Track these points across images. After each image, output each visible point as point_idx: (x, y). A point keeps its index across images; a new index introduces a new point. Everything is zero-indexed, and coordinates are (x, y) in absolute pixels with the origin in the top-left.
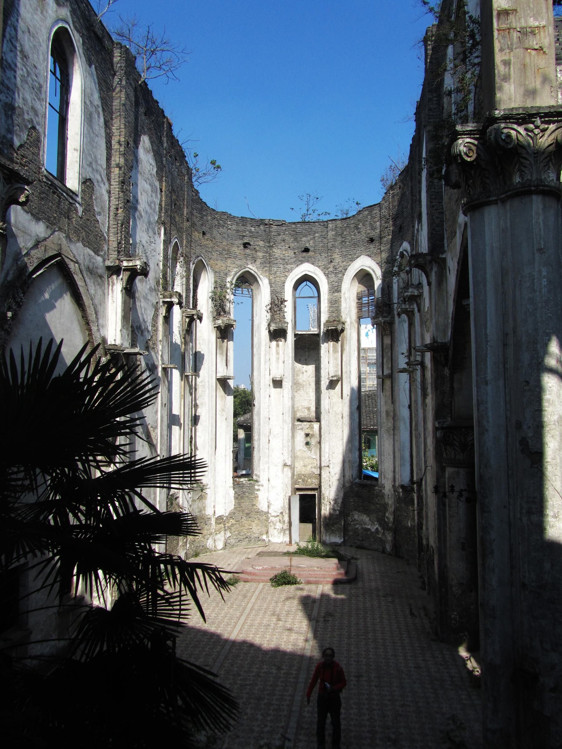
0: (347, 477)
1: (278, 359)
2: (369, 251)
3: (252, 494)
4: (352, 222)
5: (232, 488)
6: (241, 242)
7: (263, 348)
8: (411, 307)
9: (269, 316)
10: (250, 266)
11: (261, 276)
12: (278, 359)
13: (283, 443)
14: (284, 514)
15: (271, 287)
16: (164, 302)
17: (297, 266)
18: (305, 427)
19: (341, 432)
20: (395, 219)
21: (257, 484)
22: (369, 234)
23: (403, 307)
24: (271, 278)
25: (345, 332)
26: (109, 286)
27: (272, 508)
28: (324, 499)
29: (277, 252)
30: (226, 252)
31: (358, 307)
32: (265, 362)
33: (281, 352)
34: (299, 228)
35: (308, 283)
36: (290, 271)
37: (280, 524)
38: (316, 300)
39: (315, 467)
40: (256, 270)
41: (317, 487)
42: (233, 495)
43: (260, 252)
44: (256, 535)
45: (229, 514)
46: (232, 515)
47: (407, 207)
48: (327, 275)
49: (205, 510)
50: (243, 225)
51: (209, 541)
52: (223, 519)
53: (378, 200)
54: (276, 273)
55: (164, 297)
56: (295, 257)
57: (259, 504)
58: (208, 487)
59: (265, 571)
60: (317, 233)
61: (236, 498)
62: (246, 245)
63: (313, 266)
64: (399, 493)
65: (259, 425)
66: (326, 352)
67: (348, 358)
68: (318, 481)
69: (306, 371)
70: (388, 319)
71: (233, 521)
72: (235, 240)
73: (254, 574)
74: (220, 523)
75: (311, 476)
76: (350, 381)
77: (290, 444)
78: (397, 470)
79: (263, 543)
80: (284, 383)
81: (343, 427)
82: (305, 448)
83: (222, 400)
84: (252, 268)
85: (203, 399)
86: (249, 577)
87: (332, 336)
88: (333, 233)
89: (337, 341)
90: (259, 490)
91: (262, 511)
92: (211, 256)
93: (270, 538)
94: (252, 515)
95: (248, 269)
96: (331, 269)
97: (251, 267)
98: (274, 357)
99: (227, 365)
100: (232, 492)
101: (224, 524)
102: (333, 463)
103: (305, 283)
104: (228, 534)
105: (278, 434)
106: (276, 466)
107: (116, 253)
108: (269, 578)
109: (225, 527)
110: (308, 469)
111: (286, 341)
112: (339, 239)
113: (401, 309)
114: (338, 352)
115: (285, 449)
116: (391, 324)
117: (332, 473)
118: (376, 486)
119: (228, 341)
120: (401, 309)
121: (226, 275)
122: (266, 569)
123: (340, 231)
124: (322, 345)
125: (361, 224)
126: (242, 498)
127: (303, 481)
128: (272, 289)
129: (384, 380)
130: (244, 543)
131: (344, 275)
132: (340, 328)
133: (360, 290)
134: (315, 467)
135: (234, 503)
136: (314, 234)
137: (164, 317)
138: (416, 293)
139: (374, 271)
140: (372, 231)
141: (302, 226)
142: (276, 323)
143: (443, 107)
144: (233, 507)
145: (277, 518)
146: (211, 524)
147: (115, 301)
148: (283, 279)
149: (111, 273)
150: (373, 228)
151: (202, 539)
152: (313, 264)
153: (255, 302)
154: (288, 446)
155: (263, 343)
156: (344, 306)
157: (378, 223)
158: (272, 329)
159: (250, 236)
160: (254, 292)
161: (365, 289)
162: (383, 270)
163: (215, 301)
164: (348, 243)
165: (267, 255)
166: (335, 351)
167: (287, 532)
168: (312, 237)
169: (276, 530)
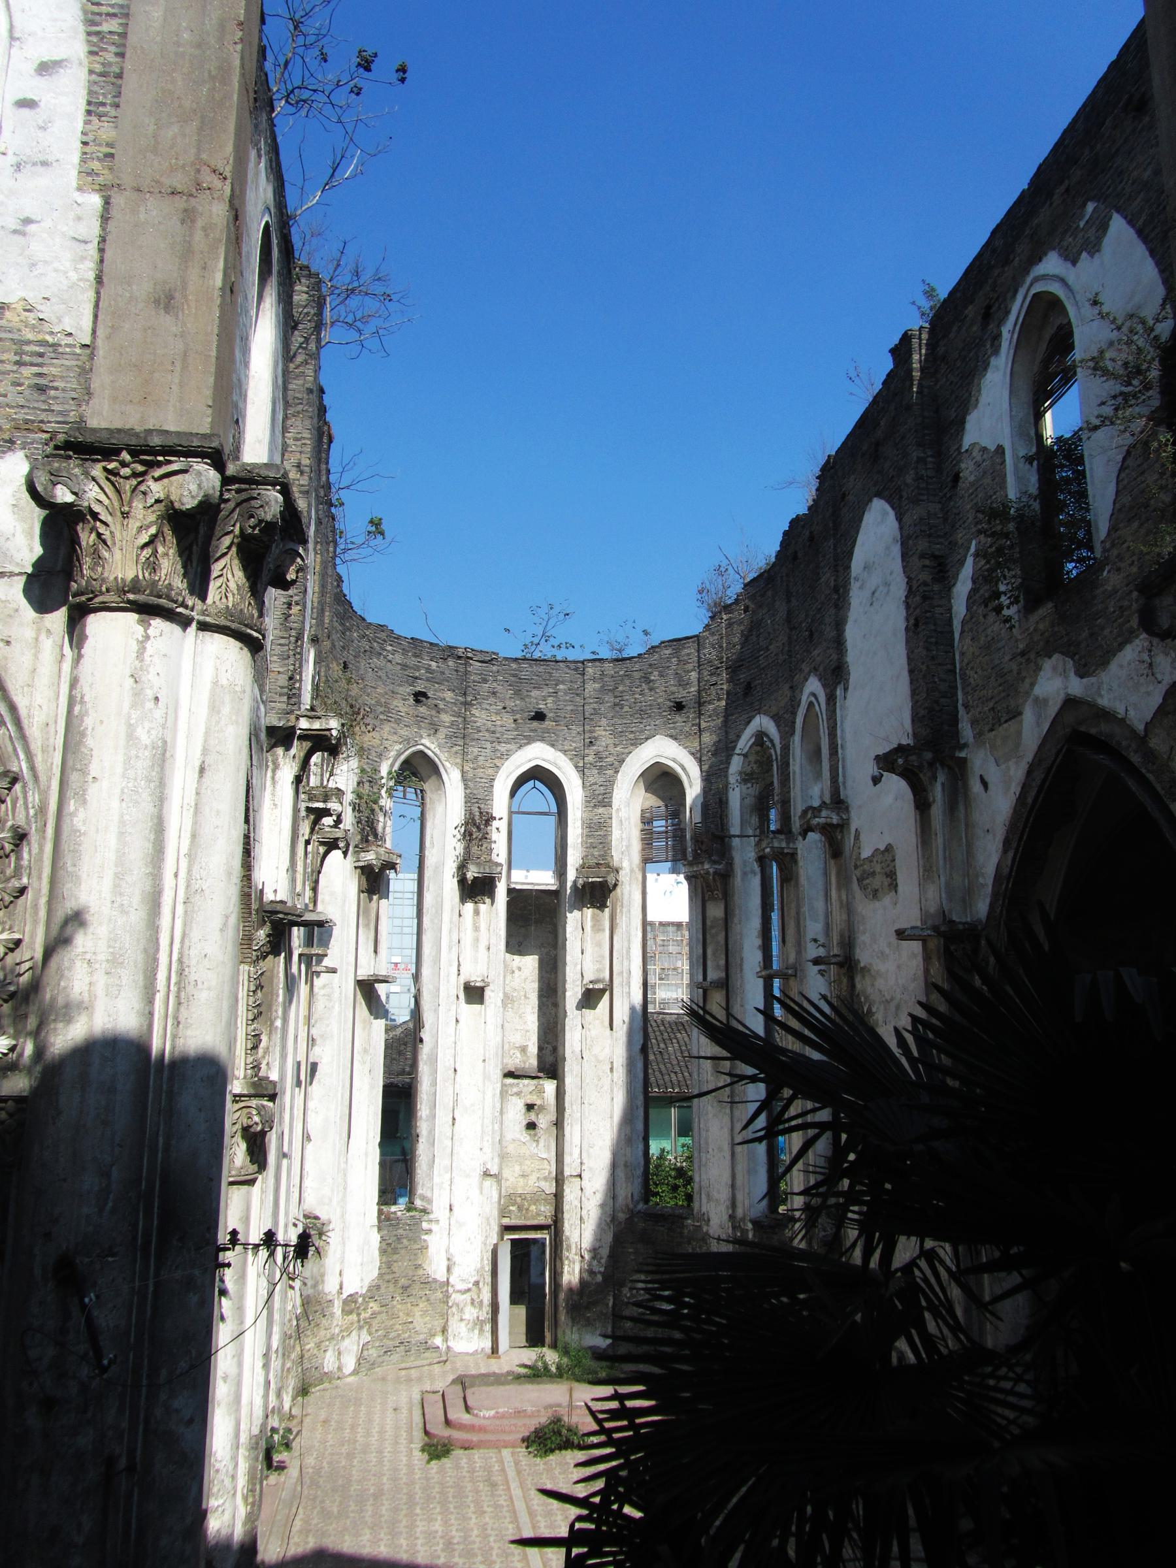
0: (620, 1200)
1: (477, 940)
2: (674, 728)
3: (415, 1242)
4: (637, 667)
5: (376, 1229)
6: (409, 689)
7: (446, 917)
8: (791, 845)
9: (460, 848)
10: (426, 741)
12: (477, 940)
13: (482, 1126)
14: (481, 1284)
15: (466, 787)
16: (309, 809)
17: (520, 747)
18: (525, 1090)
19: (609, 1100)
20: (734, 669)
21: (425, 1218)
22: (673, 693)
23: (776, 844)
25: (618, 889)
26: (267, 770)
27: (456, 1271)
28: (569, 1248)
29: (480, 716)
30: (381, 709)
31: (643, 840)
32: (450, 948)
33: (483, 926)
34: (526, 670)
35: (539, 784)
36: (506, 756)
37: (472, 1309)
38: (552, 821)
39: (545, 1179)
40: (437, 751)
41: (550, 1222)
42: (378, 1245)
43: (446, 713)
44: (422, 1337)
45: (368, 1291)
46: (374, 1291)
47: (767, 649)
48: (582, 771)
49: (323, 1282)
50: (415, 656)
51: (329, 1354)
52: (356, 1302)
53: (696, 628)
54: (476, 758)
55: (310, 800)
56: (516, 730)
57: (430, 1264)
58: (331, 1227)
59: (506, 1422)
60: (563, 682)
61: (383, 1252)
62: (419, 697)
63: (552, 750)
64: (746, 1231)
65: (434, 1083)
66: (576, 928)
67: (626, 944)
68: (552, 1209)
69: (520, 969)
70: (720, 867)
71: (374, 1306)
72: (401, 686)
73: (482, 1429)
74: (351, 1312)
75: (535, 1198)
76: (629, 993)
77: (497, 1127)
78: (739, 1182)
79: (435, 1355)
80: (488, 993)
81: (612, 1091)
82: (525, 1136)
83: (364, 1029)
84: (430, 745)
85: (328, 1025)
86: (474, 1437)
87: (592, 896)
88: (597, 686)
89: (602, 906)
90: (429, 1231)
91: (435, 1281)
93: (449, 1344)
94: (416, 1290)
95: (421, 747)
96: (590, 759)
97: (428, 744)
98: (468, 936)
99: (376, 952)
100: (375, 1238)
101: (359, 1315)
102: (591, 1169)
103: (531, 784)
104: (365, 1337)
105: (472, 1105)
106: (468, 1176)
107: (285, 699)
108: (521, 1437)
109: (359, 1321)
110: (531, 1182)
111: (493, 903)
112: (609, 699)
113: (772, 848)
114: (603, 930)
115: (486, 1138)
116: (726, 876)
117: (588, 1191)
118: (686, 1218)
119: (380, 898)
120: (772, 848)
121: (380, 755)
122: (503, 1416)
123: (610, 685)
124: (568, 915)
125: (656, 673)
126: (395, 1251)
127: (520, 1208)
128: (468, 791)
129: (708, 992)
130: (395, 1357)
131: (617, 772)
132: (611, 880)
133: (648, 804)
134: (545, 1179)
135: (378, 1264)
136: (556, 685)
138: (835, 820)
139: (684, 769)
140: (681, 689)
141: (531, 666)
142: (478, 865)
143: (956, 478)
144: (376, 1273)
145: (467, 1296)
146: (332, 1315)
147: (279, 804)
148: (490, 771)
149: (273, 741)
150: (683, 684)
151: (315, 1351)
152: (553, 746)
153: (429, 816)
154: (493, 1131)
155: (447, 906)
156: (616, 834)
157: (694, 675)
158: (470, 876)
159: (428, 680)
160: (429, 795)
161: (661, 803)
162: (705, 767)
163: (359, 811)
164: (626, 709)
165: (460, 720)
166: (597, 927)
167: (488, 1327)
168: (551, 690)
169: (463, 1324)
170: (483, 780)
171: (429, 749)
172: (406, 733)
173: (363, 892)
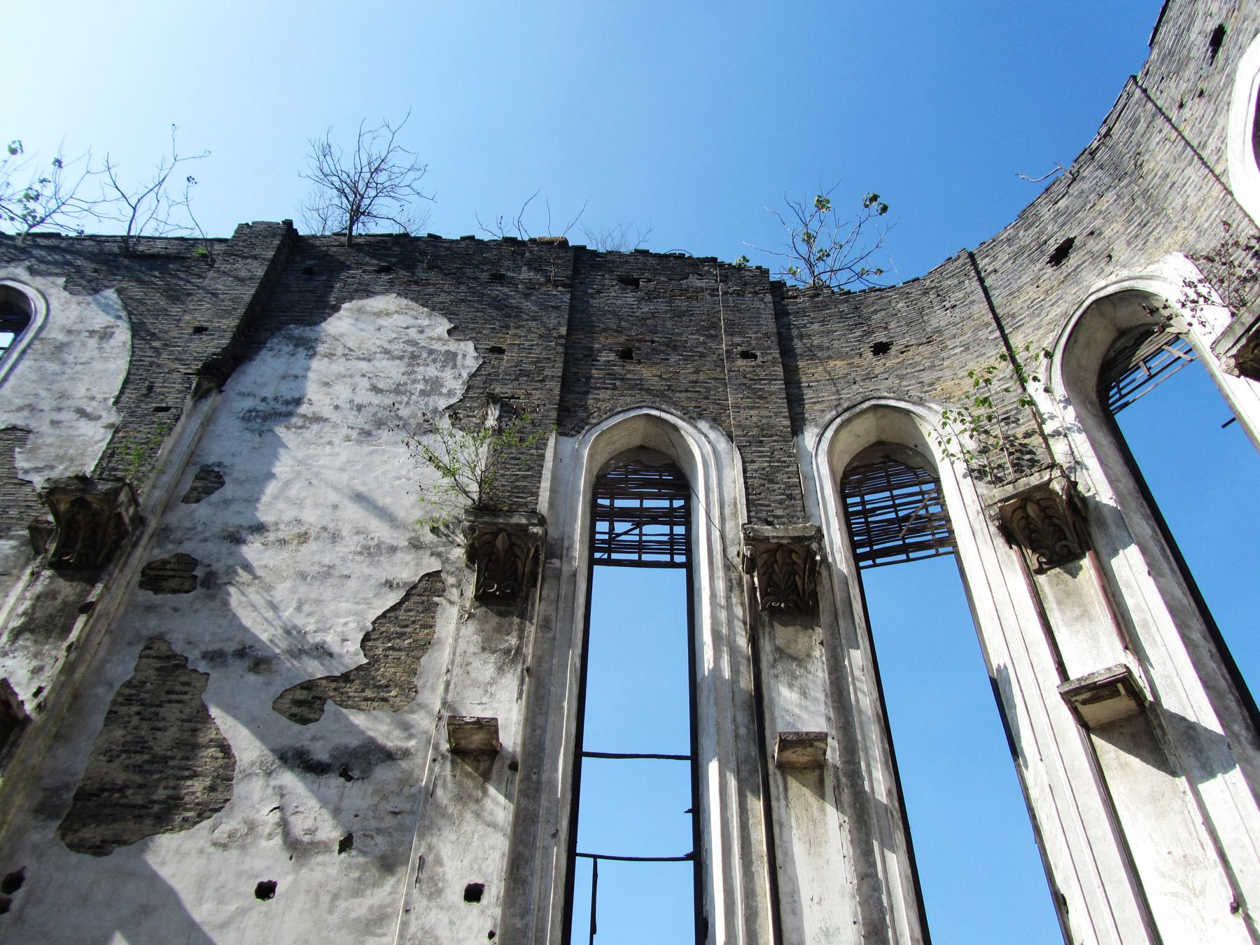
11: (1150, 268)
24: (1179, 236)
62: (1061, 254)
92: (939, 374)
97: (1102, 283)
137: (477, 597)
170: (1213, 217)
171: (1106, 286)
172: (1059, 310)
173: (1040, 571)
